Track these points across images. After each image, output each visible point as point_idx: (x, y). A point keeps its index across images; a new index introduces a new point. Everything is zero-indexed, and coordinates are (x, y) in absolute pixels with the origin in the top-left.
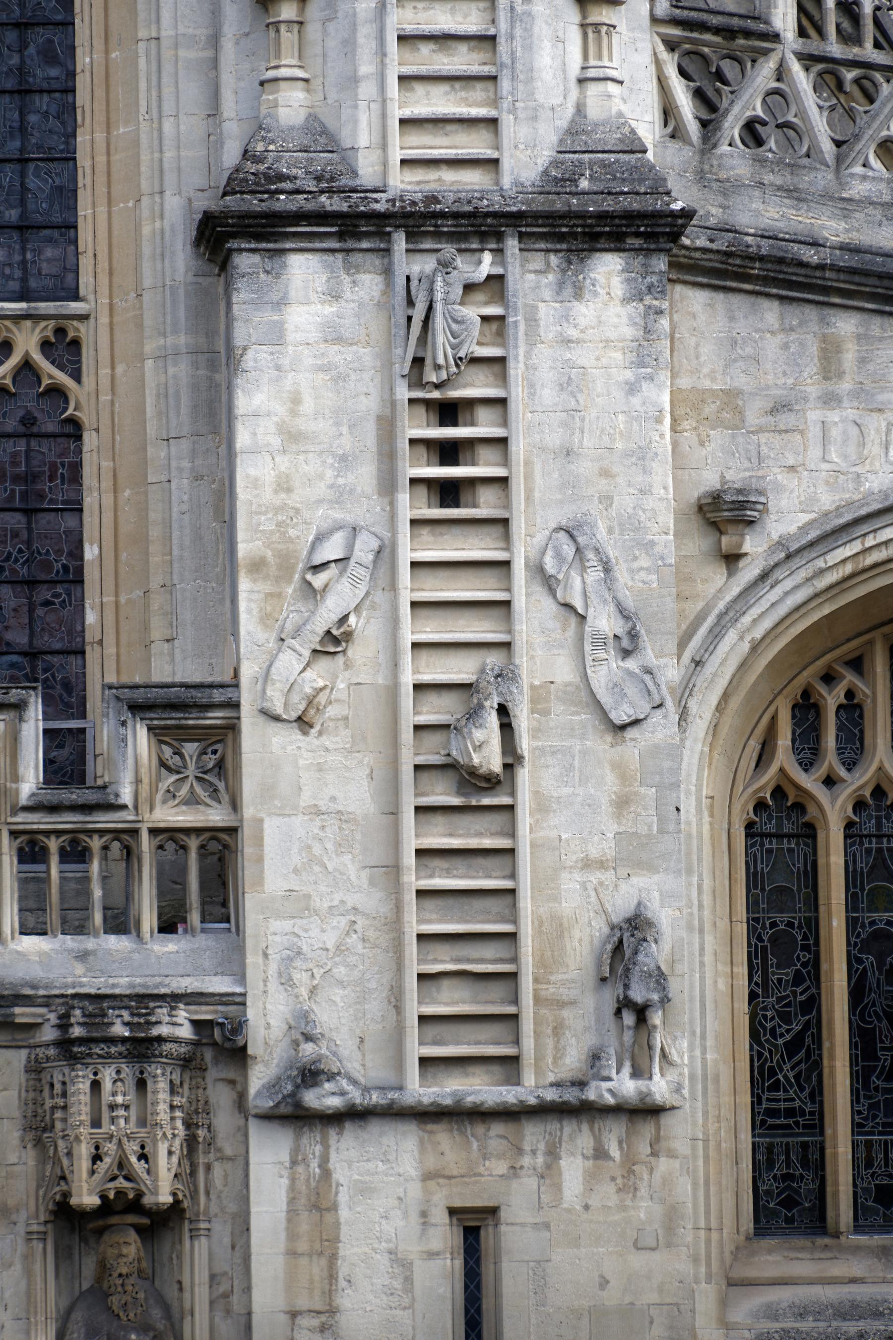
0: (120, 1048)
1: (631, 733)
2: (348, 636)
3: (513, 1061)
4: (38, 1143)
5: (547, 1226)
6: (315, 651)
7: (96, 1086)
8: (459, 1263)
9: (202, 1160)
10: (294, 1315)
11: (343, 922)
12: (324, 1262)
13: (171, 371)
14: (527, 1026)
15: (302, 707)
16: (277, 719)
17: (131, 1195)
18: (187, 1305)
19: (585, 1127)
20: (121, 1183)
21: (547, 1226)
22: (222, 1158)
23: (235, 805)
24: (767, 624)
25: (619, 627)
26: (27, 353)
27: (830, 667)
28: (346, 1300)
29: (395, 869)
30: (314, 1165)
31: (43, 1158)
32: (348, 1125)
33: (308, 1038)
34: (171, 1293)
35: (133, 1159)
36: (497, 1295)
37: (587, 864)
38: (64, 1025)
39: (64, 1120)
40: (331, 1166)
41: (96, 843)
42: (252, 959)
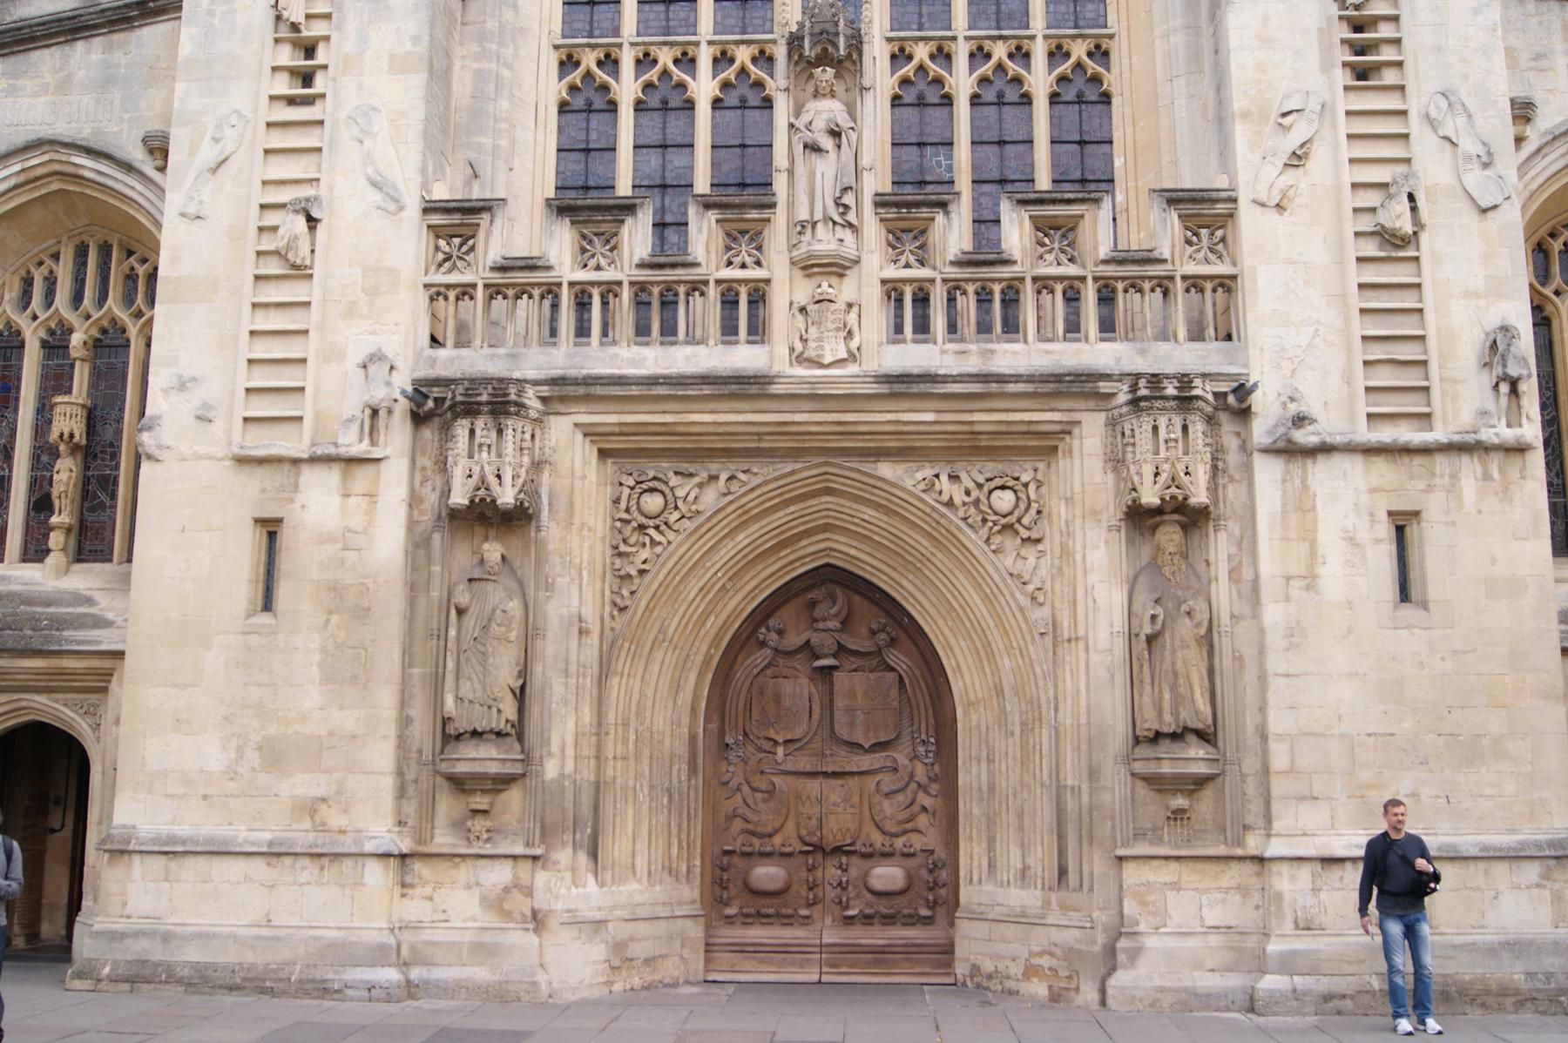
0: (1173, 403)
1: (1490, 215)
2: (1306, 155)
3: (1427, 416)
4: (1115, 469)
5: (1453, 523)
6: (1286, 165)
7: (1155, 429)
8: (1394, 547)
9: (1221, 481)
10: (1288, 579)
11: (1311, 330)
12: (1307, 544)
13: (1172, 40)
14: (1436, 393)
15: (1279, 198)
16: (1263, 205)
17: (1180, 498)
18: (1213, 574)
19: (1476, 459)
20: (1173, 490)
21: (1453, 523)
22: (1232, 479)
23: (1234, 264)
24: (1539, 181)
25: (1481, 150)
26: (1079, 57)
27: (1554, 228)
28: (1322, 571)
29: (1344, 297)
30: (1297, 482)
31: (1119, 478)
32: (1319, 457)
33: (1292, 399)
34: (1201, 567)
35: (1182, 474)
36: (1422, 568)
37: (1468, 295)
38: (1134, 388)
39: (1134, 453)
40: (1309, 483)
41: (1147, 286)
42: (1253, 353)
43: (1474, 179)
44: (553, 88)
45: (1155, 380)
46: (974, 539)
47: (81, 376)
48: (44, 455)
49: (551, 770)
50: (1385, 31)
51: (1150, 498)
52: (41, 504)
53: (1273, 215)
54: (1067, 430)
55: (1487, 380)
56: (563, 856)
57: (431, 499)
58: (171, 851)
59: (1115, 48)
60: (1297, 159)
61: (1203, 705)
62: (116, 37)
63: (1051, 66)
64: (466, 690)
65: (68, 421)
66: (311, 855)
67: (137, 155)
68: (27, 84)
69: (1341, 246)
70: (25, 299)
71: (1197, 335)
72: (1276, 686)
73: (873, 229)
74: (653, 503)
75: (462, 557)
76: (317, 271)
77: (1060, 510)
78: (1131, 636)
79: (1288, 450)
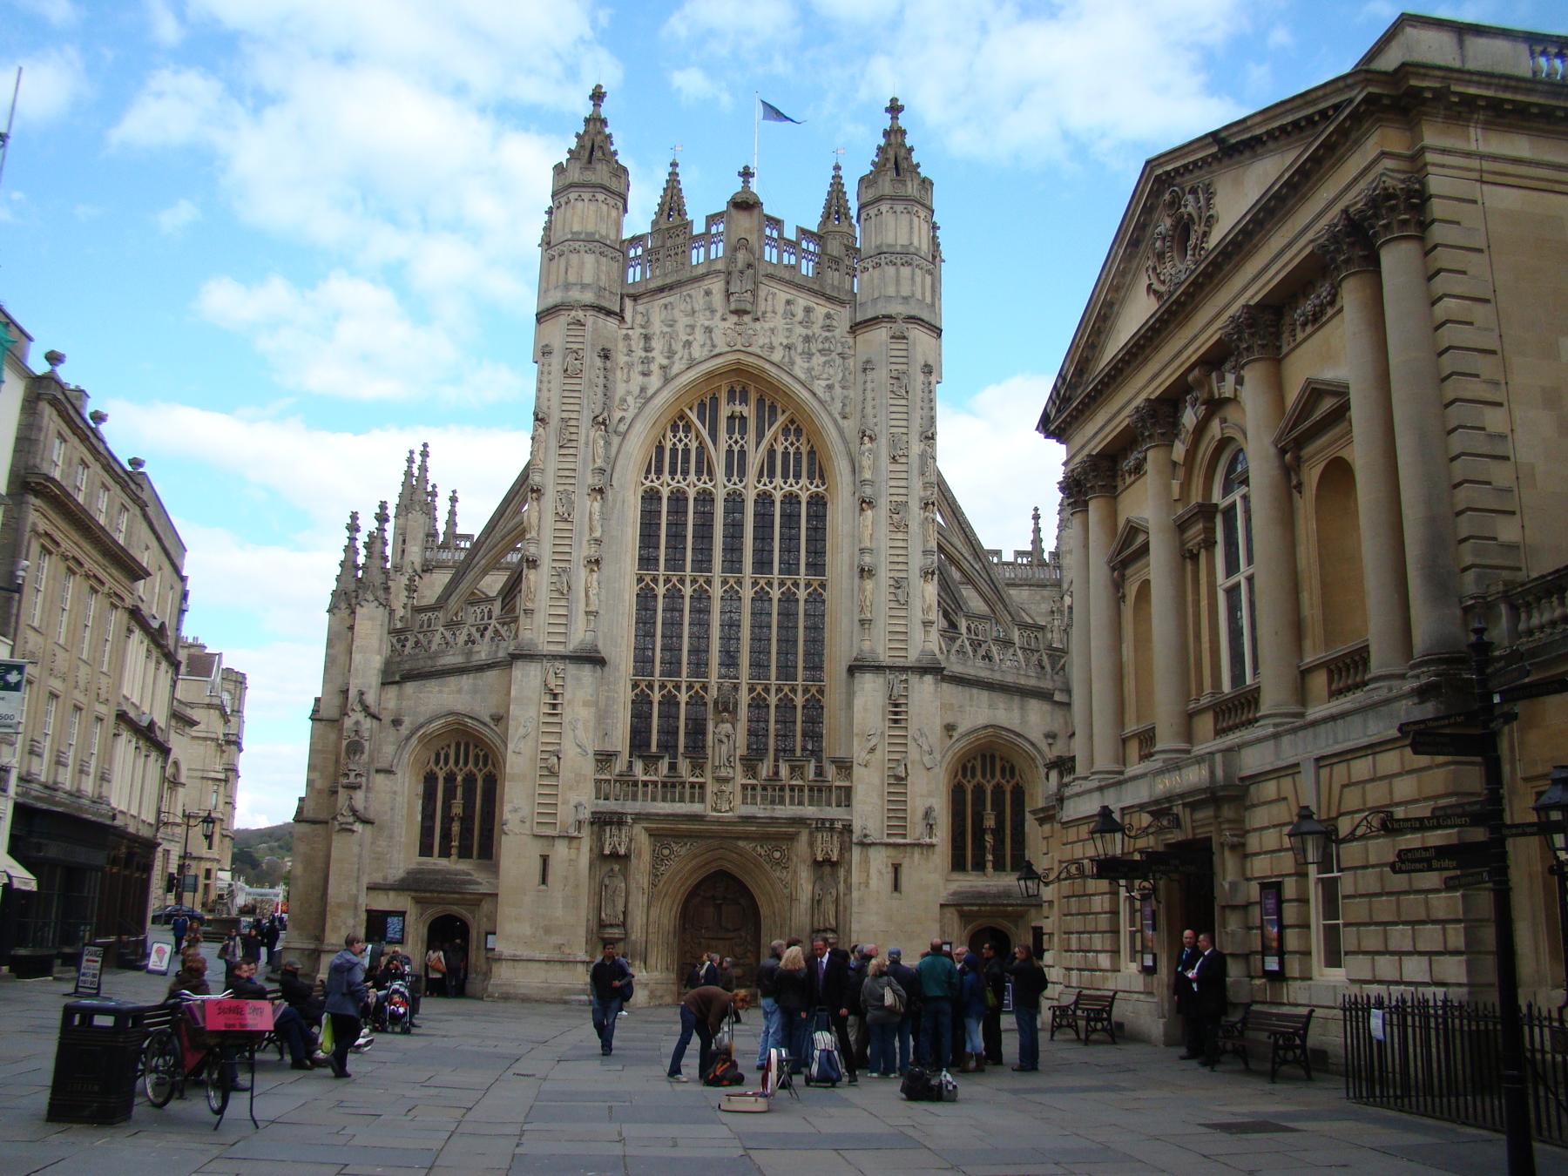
43: (926, 758)
44: (630, 695)
45: (823, 820)
46: (768, 867)
47: (459, 792)
48: (448, 819)
49: (633, 937)
50: (903, 709)
51: (820, 858)
52: (446, 836)
53: (863, 769)
54: (798, 833)
55: (925, 822)
56: (637, 963)
57: (596, 851)
58: (515, 959)
59: (827, 691)
60: (872, 750)
61: (833, 922)
62: (479, 675)
63: (804, 694)
64: (608, 912)
65: (457, 809)
66: (560, 962)
67: (487, 719)
68: (446, 689)
69: (883, 780)
70: (437, 762)
71: (839, 805)
72: (854, 918)
73: (739, 768)
74: (666, 852)
75: (606, 868)
76: (561, 775)
77: (795, 859)
78: (813, 900)
79: (862, 844)
